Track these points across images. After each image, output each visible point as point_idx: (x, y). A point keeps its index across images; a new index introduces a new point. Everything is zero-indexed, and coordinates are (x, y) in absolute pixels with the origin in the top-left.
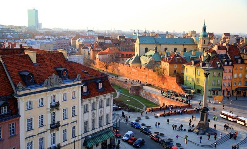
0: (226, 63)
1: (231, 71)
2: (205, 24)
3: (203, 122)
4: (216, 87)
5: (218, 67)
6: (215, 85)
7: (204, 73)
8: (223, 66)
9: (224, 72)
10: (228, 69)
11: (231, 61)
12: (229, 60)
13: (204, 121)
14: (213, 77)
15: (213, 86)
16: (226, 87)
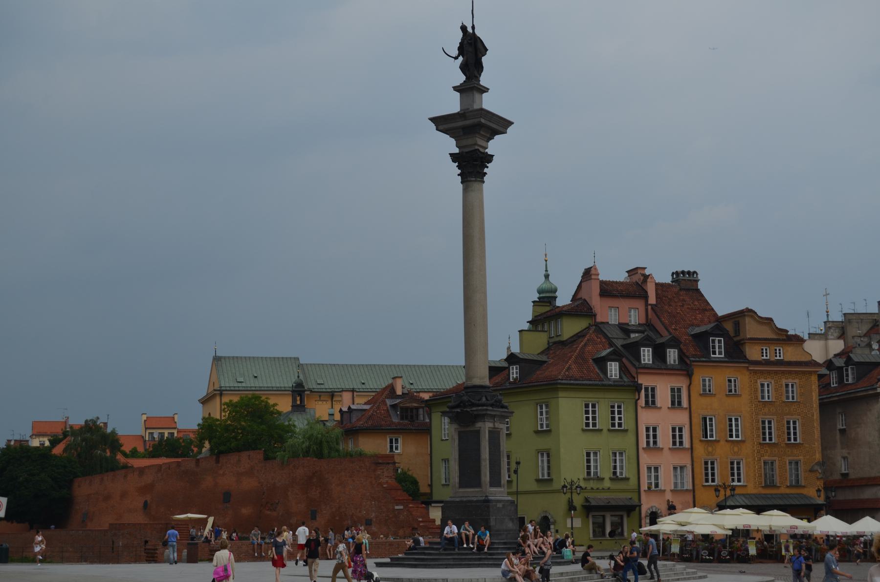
0: (647, 355)
1: (680, 403)
2: (547, 276)
3: (471, 494)
4: (607, 492)
5: (605, 373)
6: (602, 479)
7: (454, 157)
8: (633, 370)
9: (642, 402)
10: (663, 387)
11: (675, 343)
12: (660, 341)
13: (478, 484)
14: (583, 430)
15: (592, 484)
16: (665, 491)
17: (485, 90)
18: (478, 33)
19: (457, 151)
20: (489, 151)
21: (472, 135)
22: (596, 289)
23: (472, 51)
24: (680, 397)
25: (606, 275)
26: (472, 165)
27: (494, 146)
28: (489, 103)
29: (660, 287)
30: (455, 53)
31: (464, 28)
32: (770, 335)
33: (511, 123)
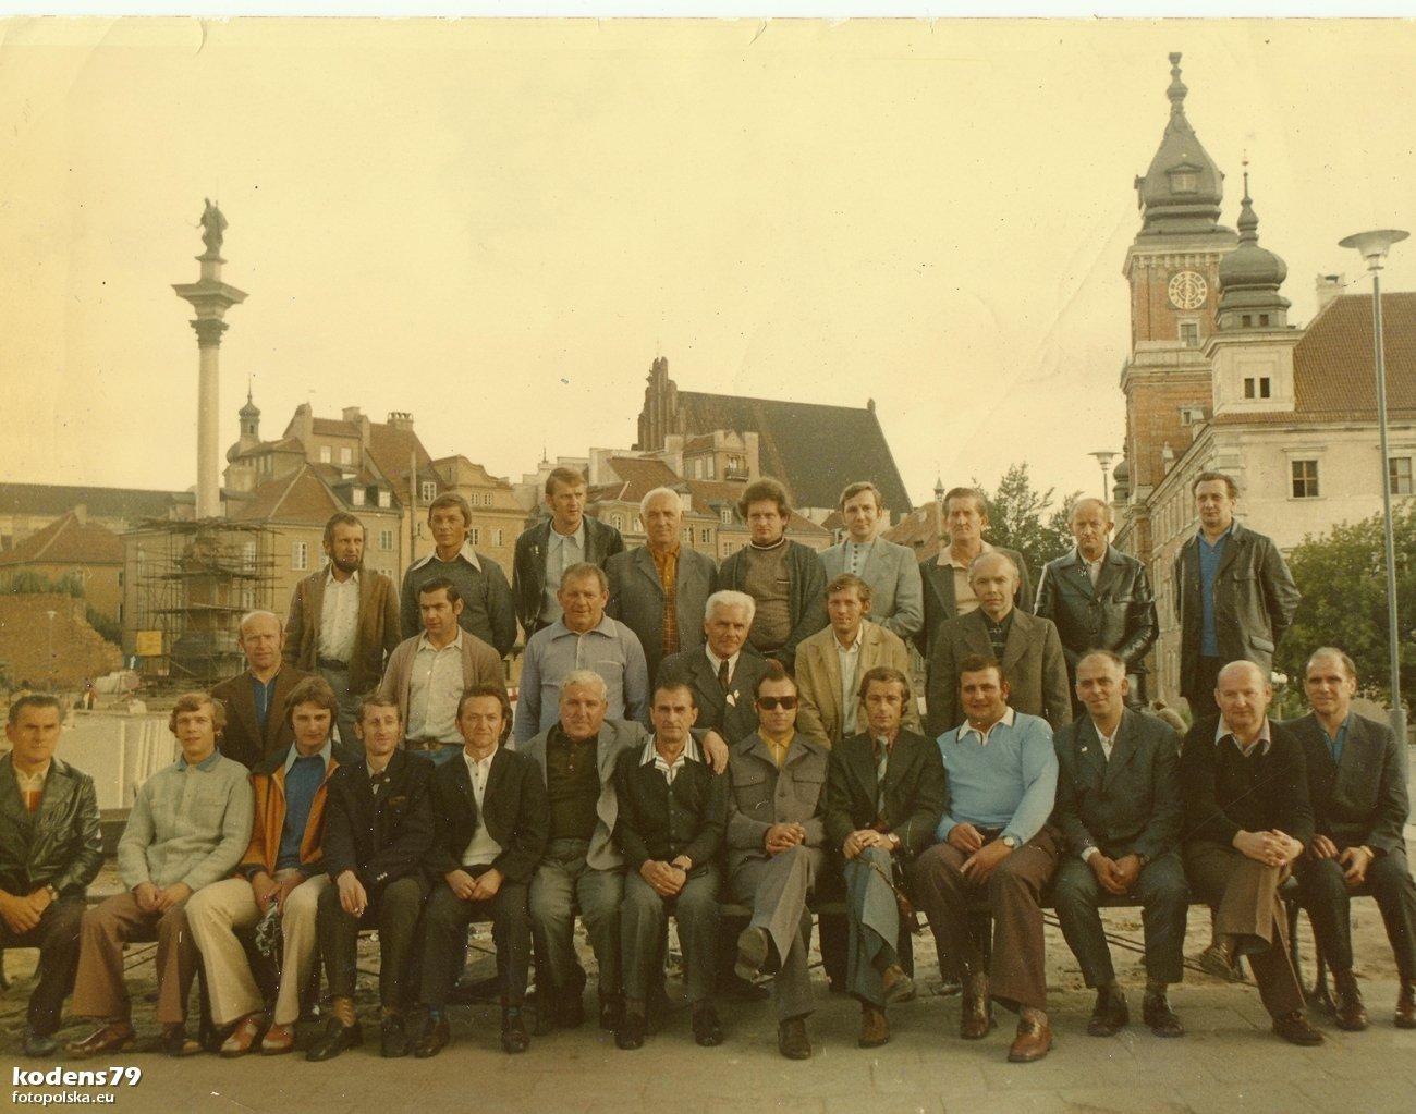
0: (359, 496)
7: (193, 324)
17: (223, 262)
18: (221, 209)
19: (195, 317)
20: (223, 320)
21: (210, 303)
22: (310, 427)
23: (213, 224)
24: (390, 540)
25: (317, 413)
26: (209, 332)
27: (230, 316)
28: (228, 275)
29: (375, 428)
30: (199, 222)
31: (207, 202)
32: (479, 481)
33: (247, 295)
